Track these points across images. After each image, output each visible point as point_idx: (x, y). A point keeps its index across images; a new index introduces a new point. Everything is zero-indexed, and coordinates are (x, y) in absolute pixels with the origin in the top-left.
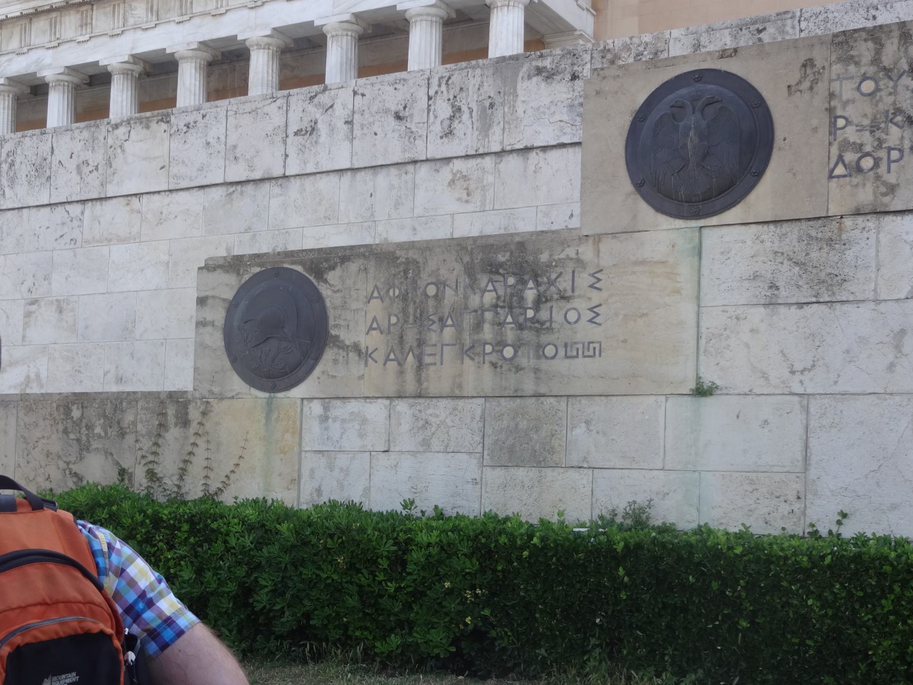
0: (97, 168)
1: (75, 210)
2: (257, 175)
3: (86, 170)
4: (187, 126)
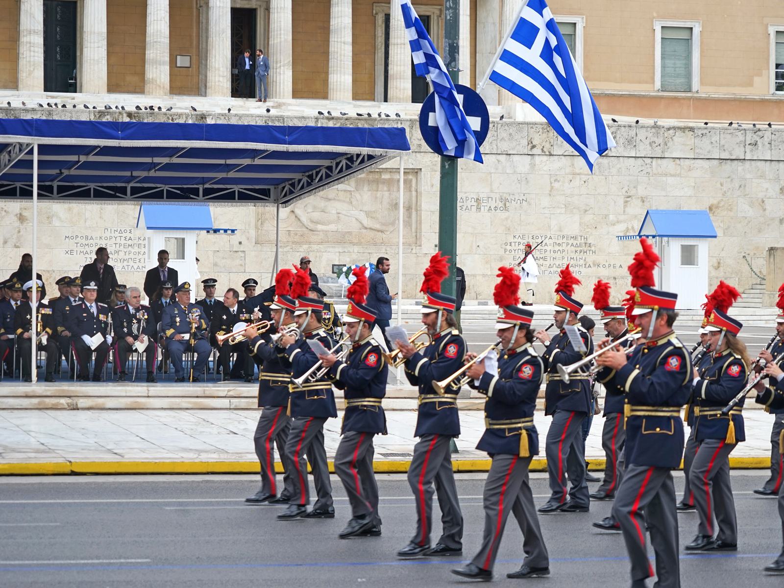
0: (660, 145)
1: (648, 161)
2: (734, 157)
3: (654, 145)
4: (702, 134)
